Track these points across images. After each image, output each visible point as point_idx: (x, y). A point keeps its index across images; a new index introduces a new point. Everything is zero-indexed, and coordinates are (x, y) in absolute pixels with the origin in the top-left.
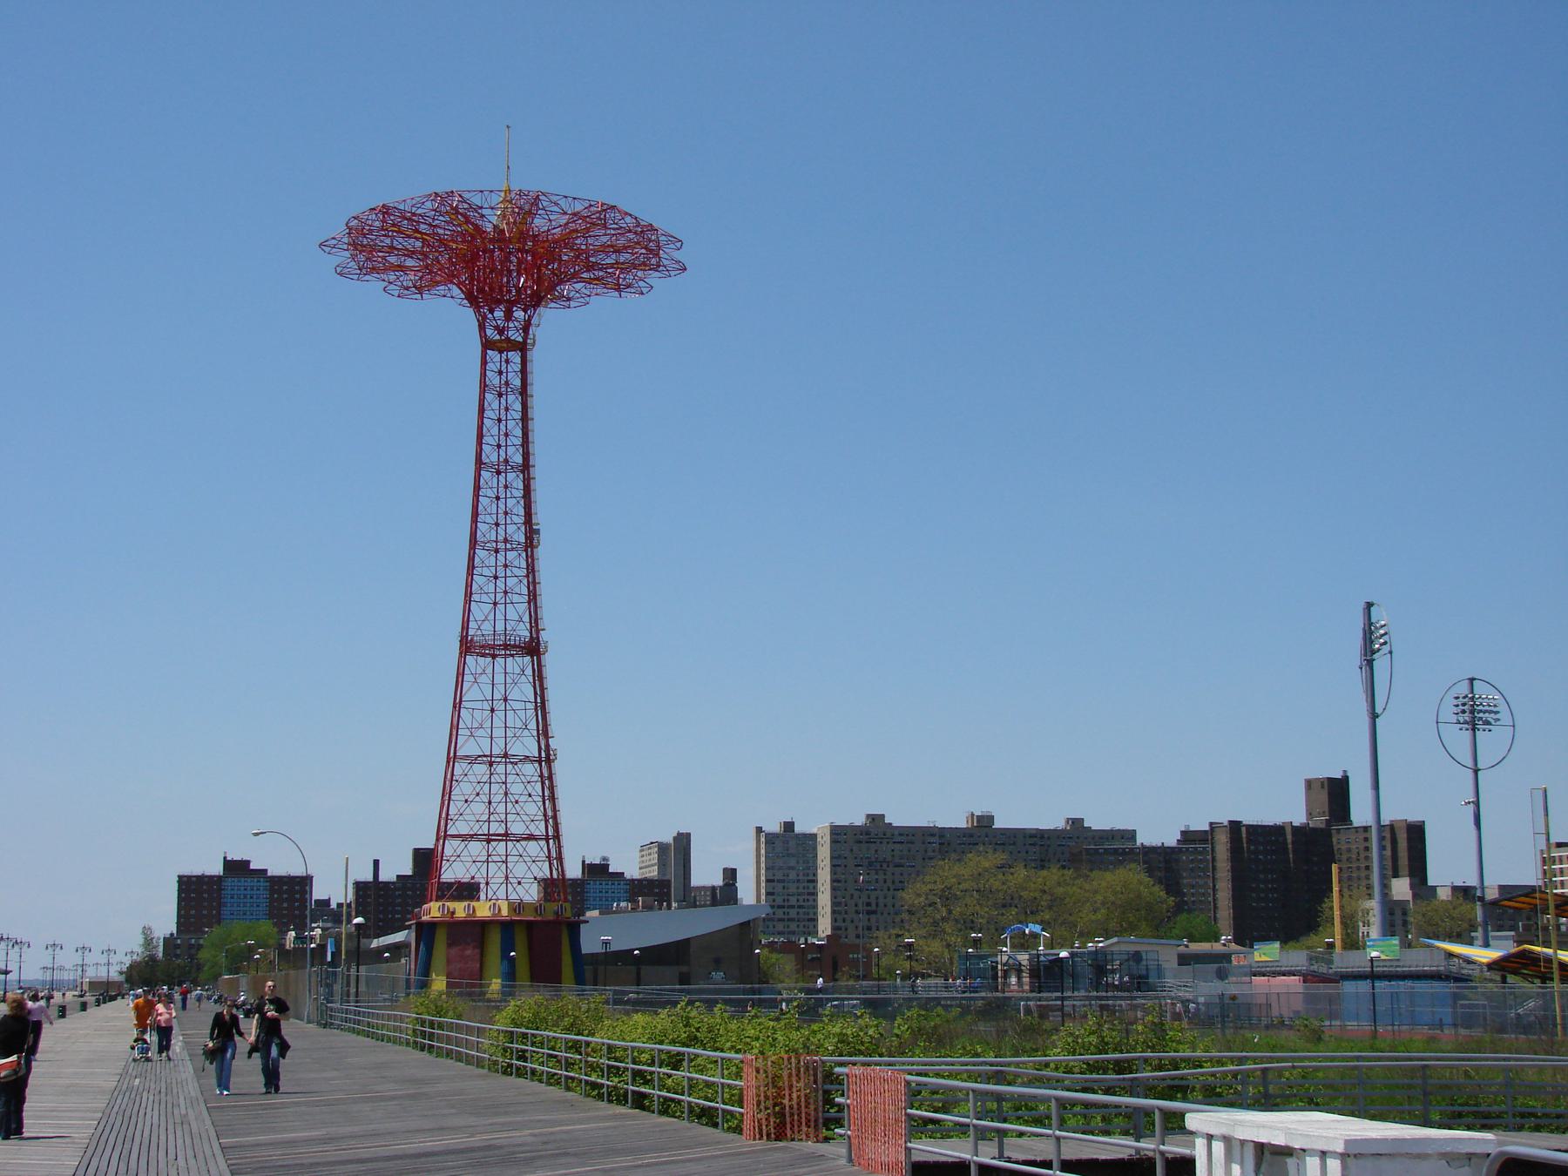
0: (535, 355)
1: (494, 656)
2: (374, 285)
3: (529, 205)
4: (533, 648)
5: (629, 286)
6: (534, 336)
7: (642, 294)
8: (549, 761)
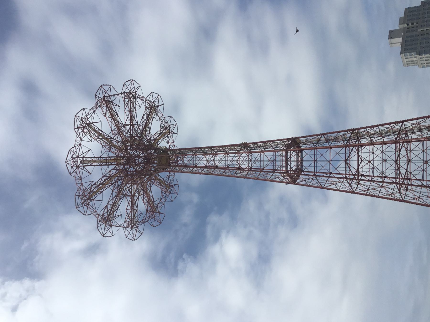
7: (176, 124)
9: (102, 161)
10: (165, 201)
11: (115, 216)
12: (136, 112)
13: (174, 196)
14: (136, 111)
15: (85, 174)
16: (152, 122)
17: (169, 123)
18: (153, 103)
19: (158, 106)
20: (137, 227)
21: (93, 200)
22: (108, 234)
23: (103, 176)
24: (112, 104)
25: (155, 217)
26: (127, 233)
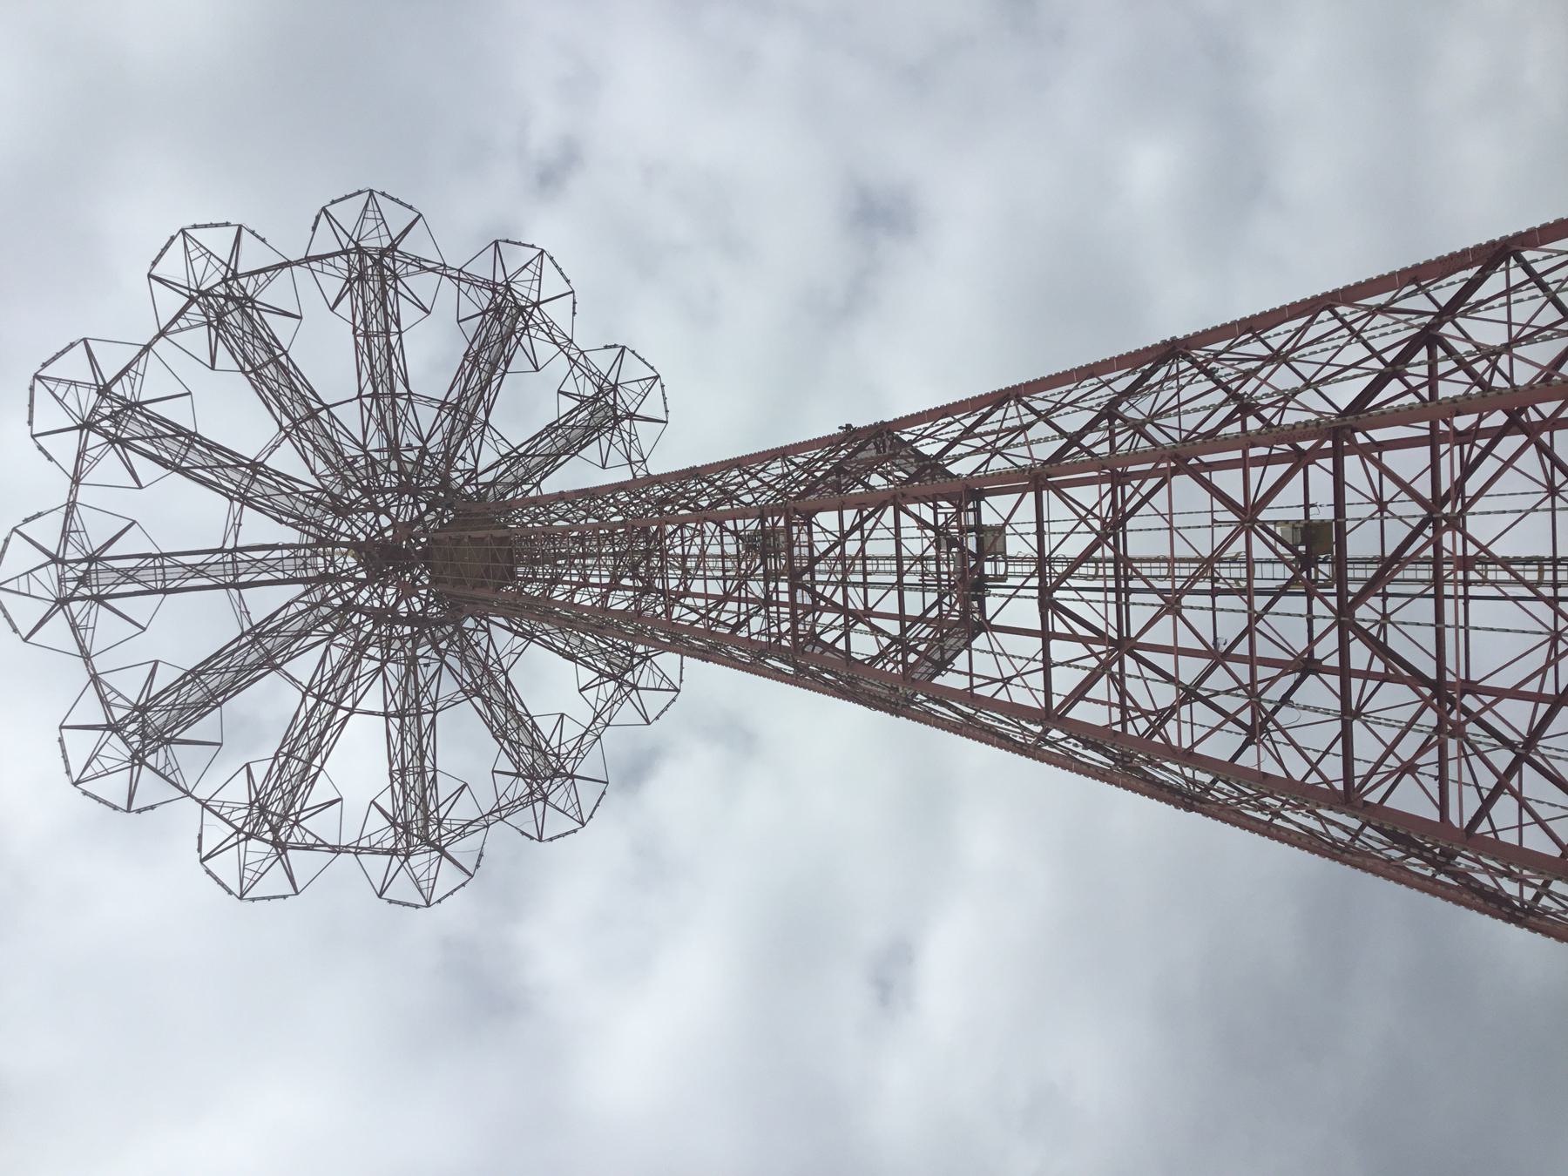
7: (657, 377)
9: (202, 571)
11: (302, 810)
12: (400, 338)
14: (400, 333)
16: (503, 375)
17: (612, 379)
18: (508, 288)
19: (536, 305)
21: (169, 742)
24: (253, 307)
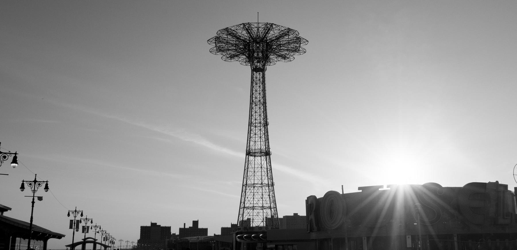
0: (267, 73)
1: (255, 156)
2: (219, 55)
3: (269, 27)
4: (267, 154)
5: (288, 58)
6: (266, 67)
7: (291, 61)
8: (273, 185)
10: (239, 61)
13: (245, 64)
15: (241, 31)
20: (218, 52)
22: (209, 42)
23: (243, 35)
25: (228, 58)
26: (212, 49)
